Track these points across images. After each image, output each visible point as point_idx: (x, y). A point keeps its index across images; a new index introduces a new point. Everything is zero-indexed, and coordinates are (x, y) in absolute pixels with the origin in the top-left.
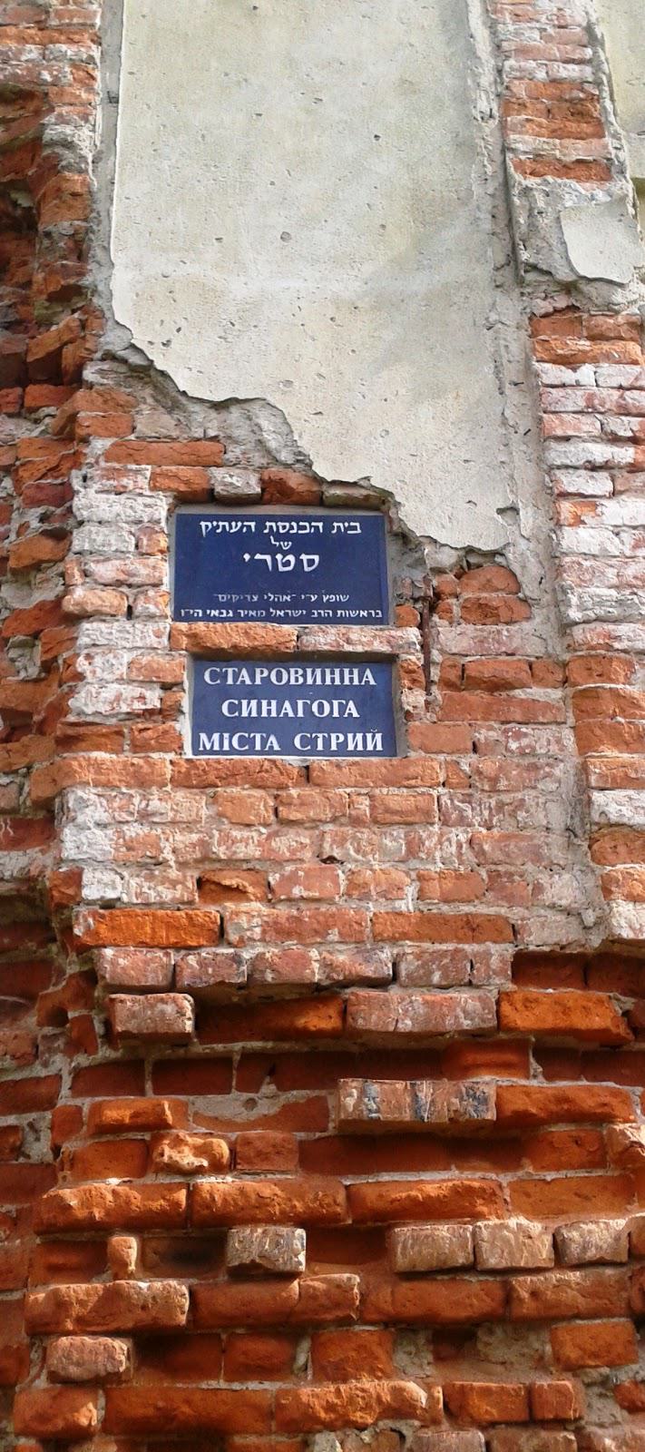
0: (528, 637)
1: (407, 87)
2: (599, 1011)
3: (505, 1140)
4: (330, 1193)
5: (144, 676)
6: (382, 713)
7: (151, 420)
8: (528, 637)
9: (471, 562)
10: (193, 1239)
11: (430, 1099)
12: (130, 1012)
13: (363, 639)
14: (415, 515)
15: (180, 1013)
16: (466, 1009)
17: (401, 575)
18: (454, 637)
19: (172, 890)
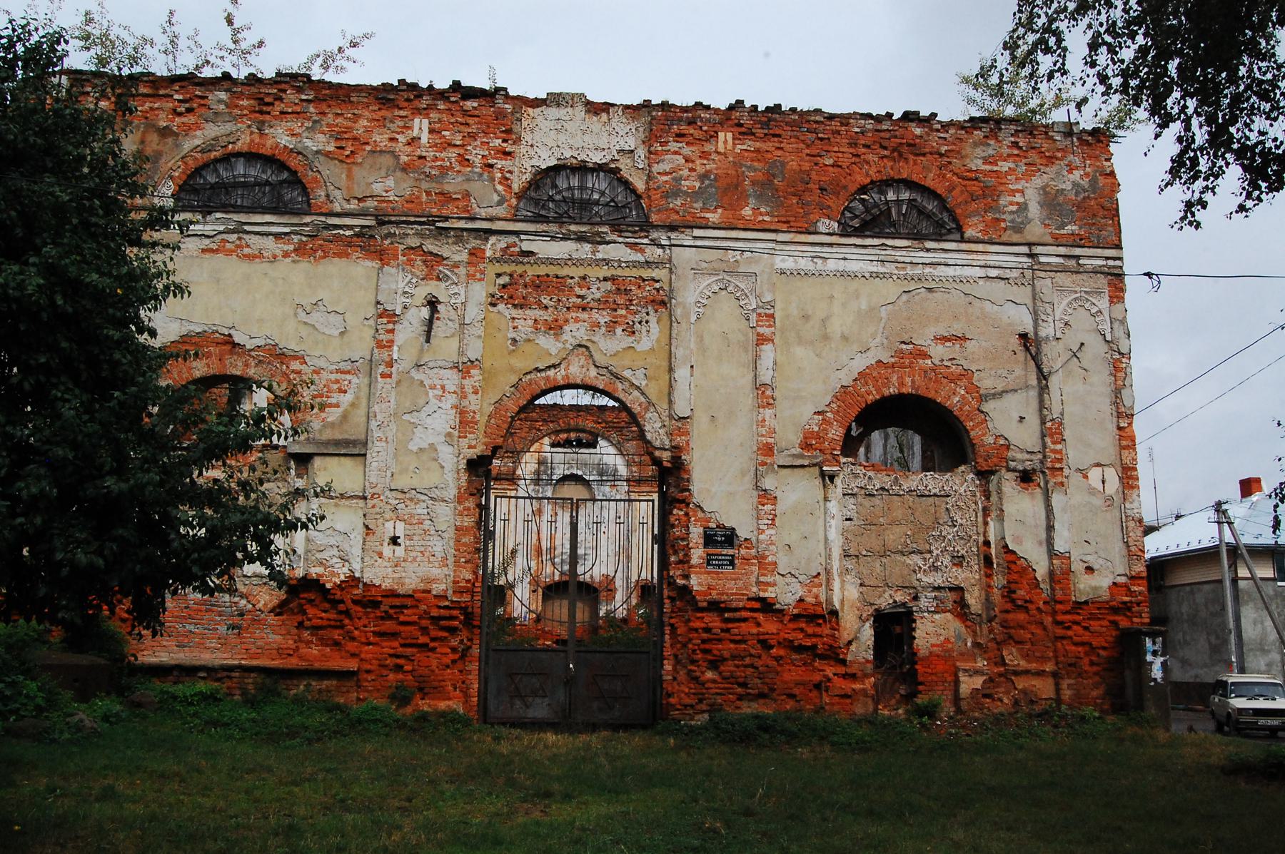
0: (753, 552)
1: (741, 445)
2: (757, 605)
3: (745, 620)
4: (724, 626)
5: (701, 557)
6: (732, 563)
7: (700, 515)
8: (753, 552)
9: (746, 540)
10: (707, 630)
11: (737, 615)
12: (700, 604)
13: (730, 552)
14: (738, 532)
15: (705, 604)
16: (741, 605)
17: (736, 542)
18: (743, 552)
19: (704, 589)
